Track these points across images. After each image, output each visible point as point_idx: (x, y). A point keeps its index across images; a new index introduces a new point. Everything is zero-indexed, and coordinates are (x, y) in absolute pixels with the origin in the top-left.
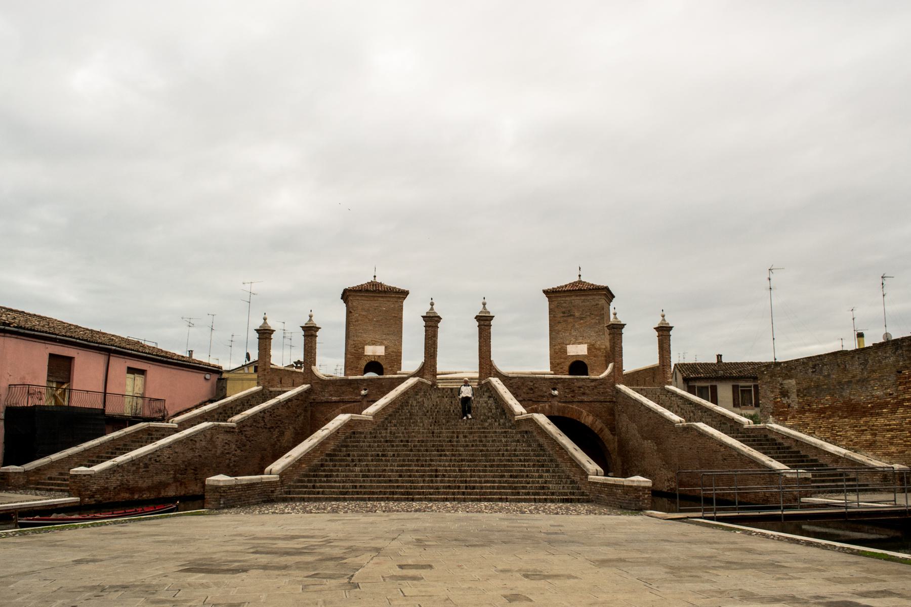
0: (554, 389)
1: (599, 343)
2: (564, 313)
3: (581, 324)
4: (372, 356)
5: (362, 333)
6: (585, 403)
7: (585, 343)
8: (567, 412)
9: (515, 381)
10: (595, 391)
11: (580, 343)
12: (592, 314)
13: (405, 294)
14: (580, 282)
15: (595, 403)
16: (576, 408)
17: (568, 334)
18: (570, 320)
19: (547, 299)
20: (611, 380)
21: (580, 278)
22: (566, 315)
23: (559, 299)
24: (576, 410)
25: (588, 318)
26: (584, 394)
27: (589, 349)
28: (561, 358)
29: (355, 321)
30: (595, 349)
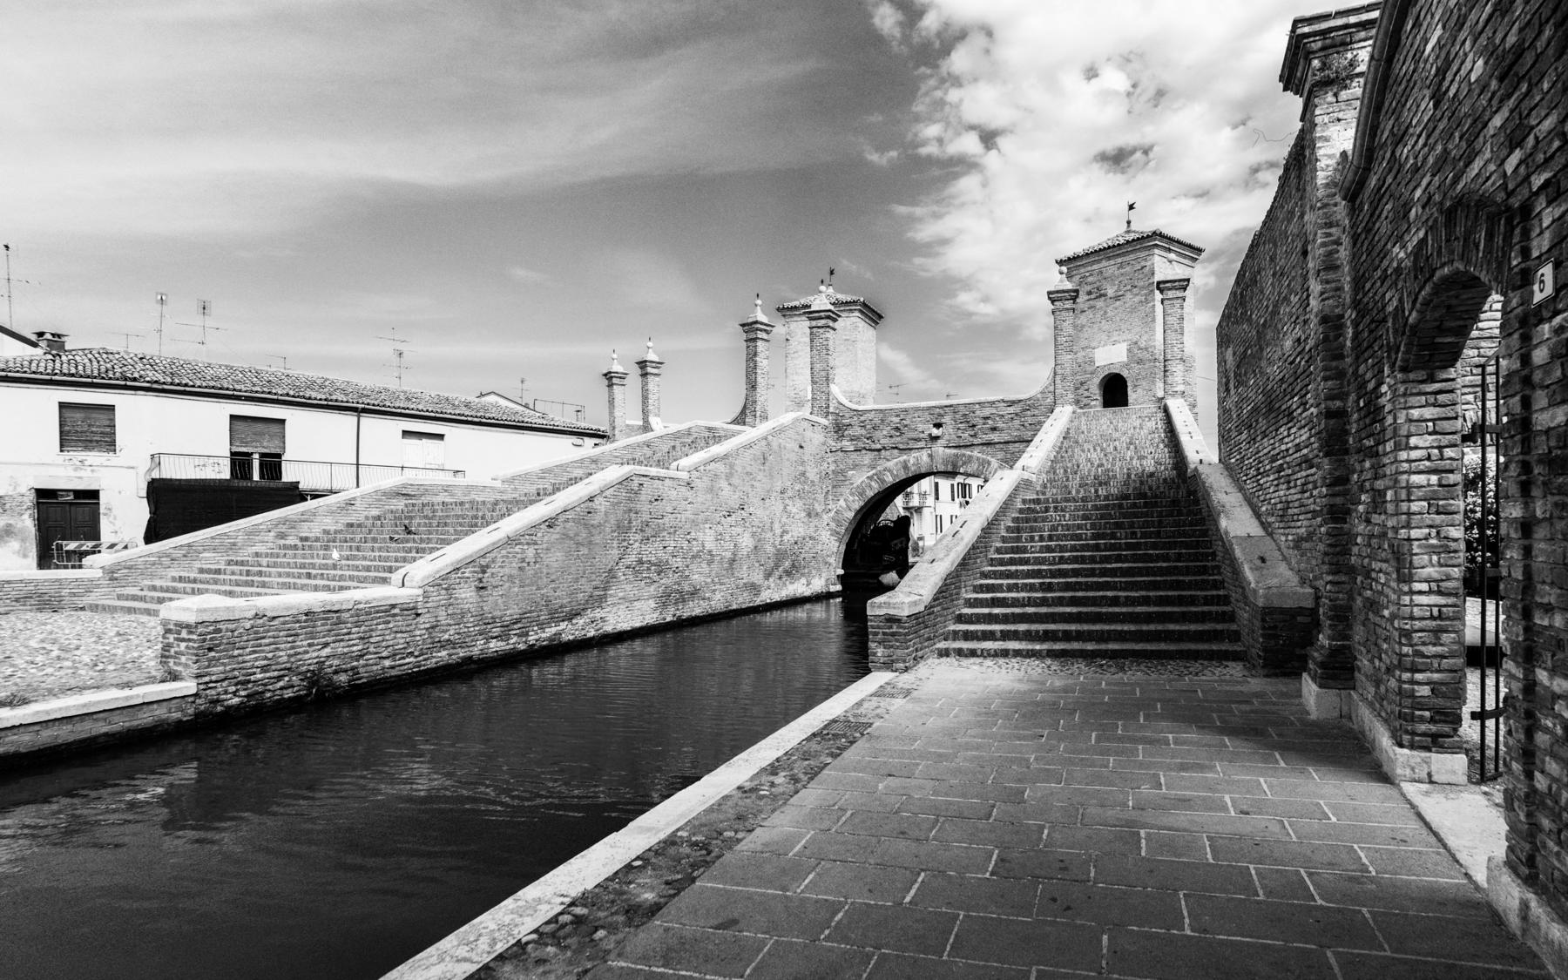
0: (938, 426)
1: (1145, 337)
6: (997, 446)
8: (960, 463)
9: (870, 416)
10: (1017, 422)
15: (1017, 445)
16: (979, 455)
17: (1096, 330)
18: (1100, 303)
20: (1049, 400)
21: (1129, 226)
22: (1092, 296)
23: (1082, 271)
24: (978, 459)
25: (1129, 295)
26: (994, 429)
27: (1129, 351)
28: (1085, 373)
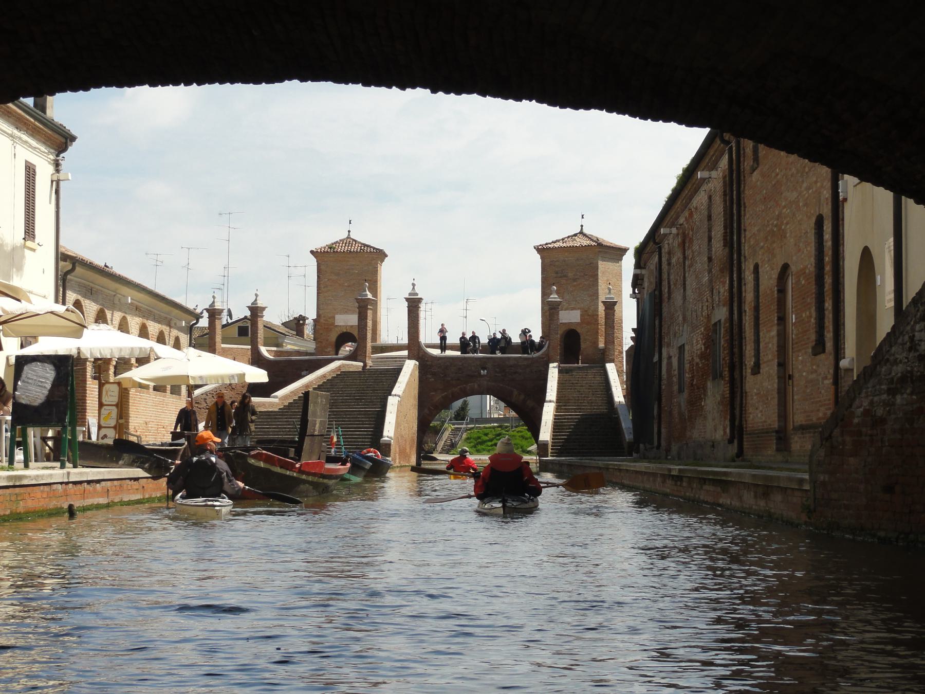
1: (592, 308)
2: (557, 273)
3: (575, 286)
4: (343, 326)
5: (331, 300)
7: (578, 309)
11: (573, 309)
12: (586, 275)
13: (380, 255)
14: (581, 233)
18: (563, 281)
19: (539, 256)
21: (582, 229)
27: (581, 315)
29: (324, 287)
30: (589, 315)
